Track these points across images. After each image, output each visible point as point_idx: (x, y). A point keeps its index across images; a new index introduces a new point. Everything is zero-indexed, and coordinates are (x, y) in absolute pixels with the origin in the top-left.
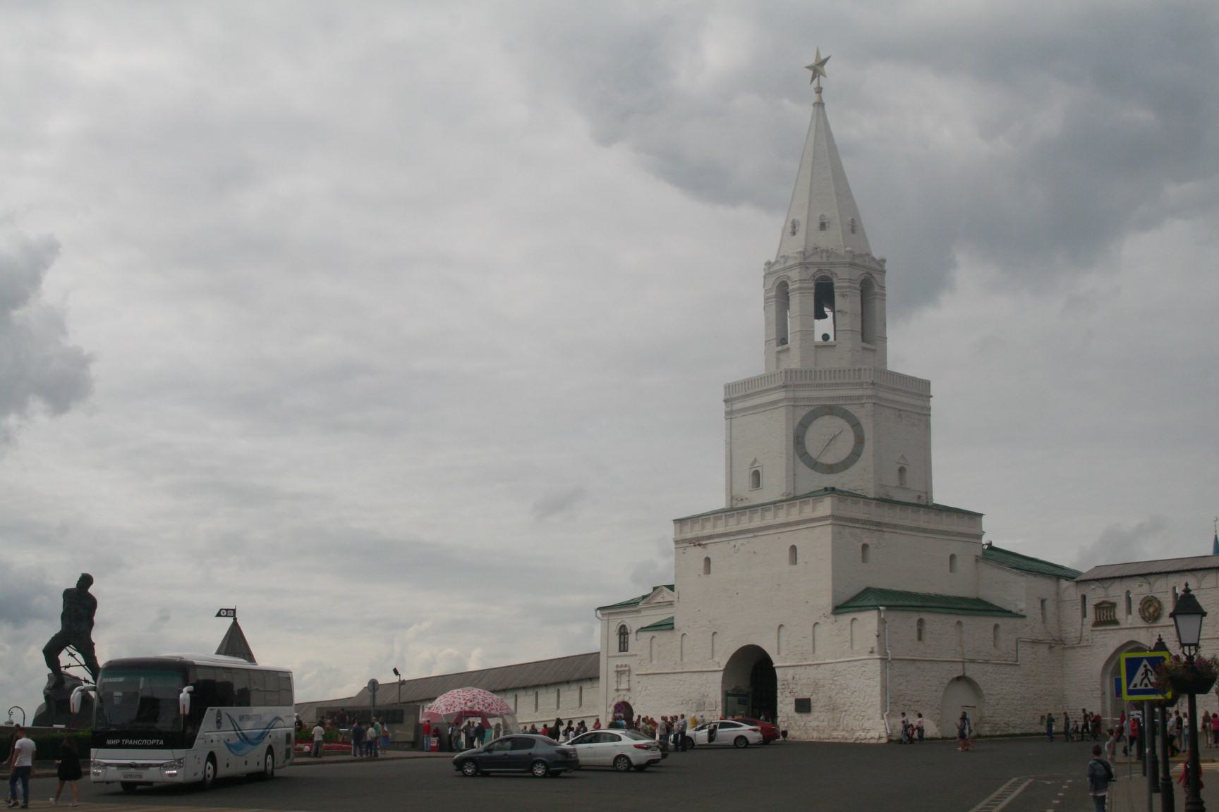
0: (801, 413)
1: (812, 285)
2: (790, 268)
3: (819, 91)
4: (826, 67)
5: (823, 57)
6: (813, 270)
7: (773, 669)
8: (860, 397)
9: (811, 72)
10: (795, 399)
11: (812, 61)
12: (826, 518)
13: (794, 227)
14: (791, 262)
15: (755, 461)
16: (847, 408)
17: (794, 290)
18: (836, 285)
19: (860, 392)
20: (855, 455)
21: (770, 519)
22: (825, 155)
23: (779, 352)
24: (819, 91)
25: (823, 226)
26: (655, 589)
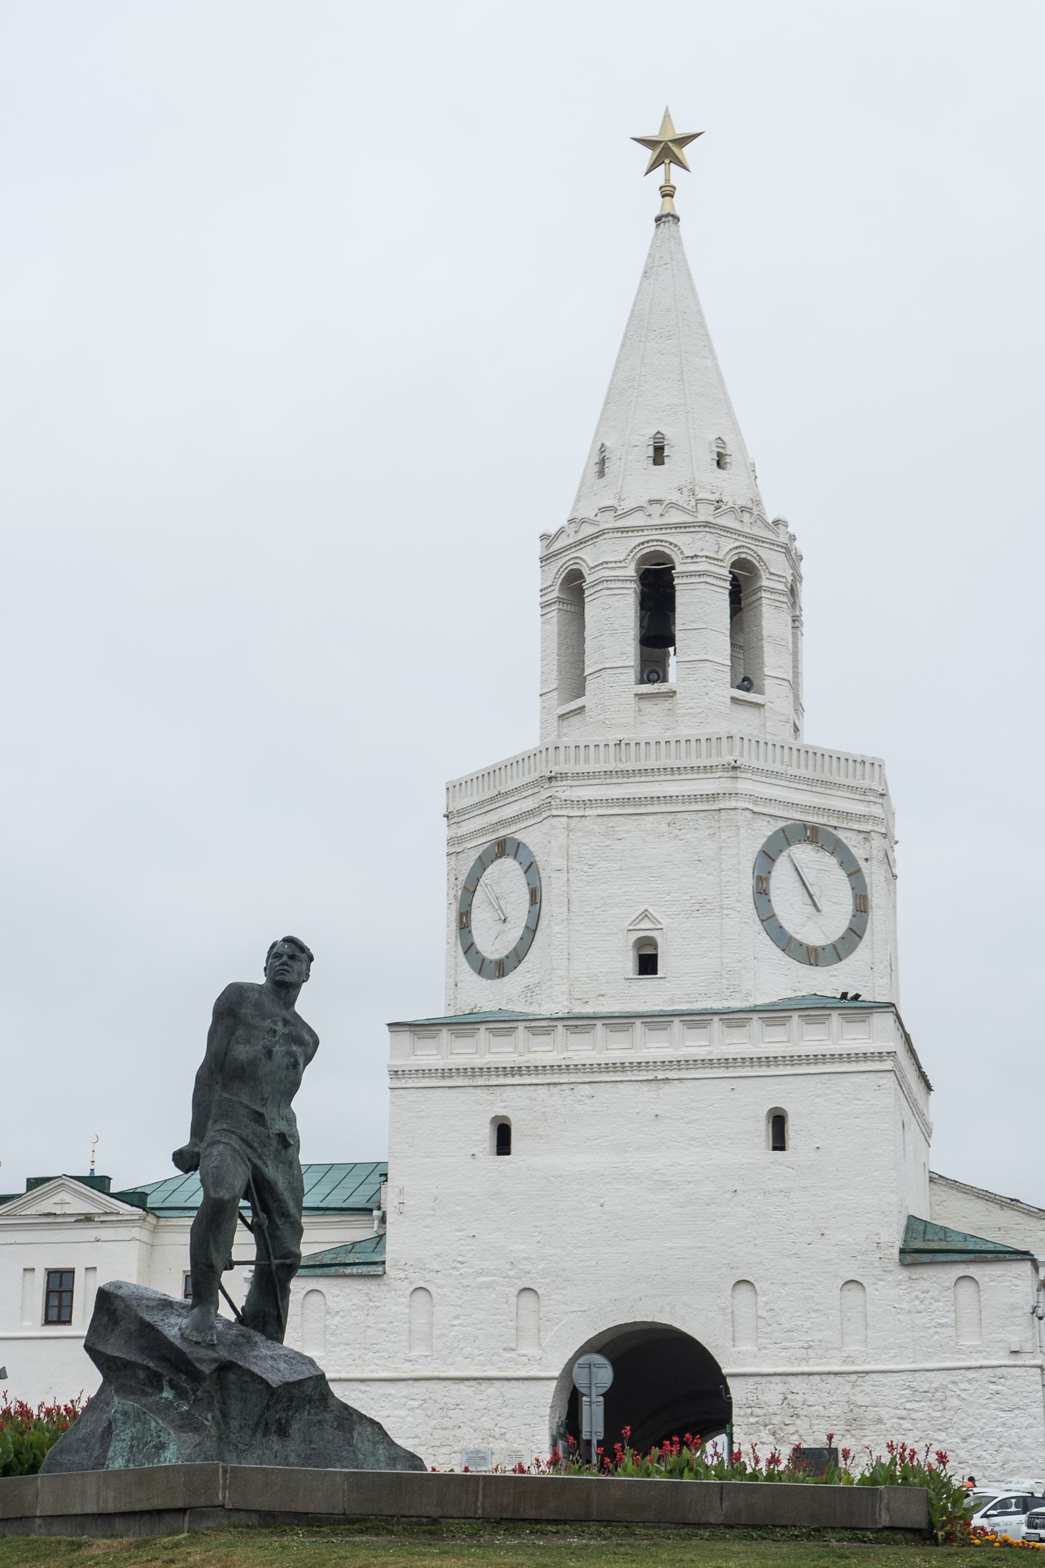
0: (767, 829)
2: (677, 526)
3: (668, 192)
4: (687, 153)
5: (681, 130)
6: (728, 544)
7: (722, 1379)
8: (862, 818)
9: (648, 155)
10: (757, 800)
11: (652, 132)
12: (880, 1056)
14: (676, 517)
15: (645, 915)
16: (841, 835)
18: (765, 583)
20: (855, 933)
21: (695, 1044)
22: (665, 321)
23: (640, 696)
24: (668, 192)
25: (720, 462)
26: (33, 1183)
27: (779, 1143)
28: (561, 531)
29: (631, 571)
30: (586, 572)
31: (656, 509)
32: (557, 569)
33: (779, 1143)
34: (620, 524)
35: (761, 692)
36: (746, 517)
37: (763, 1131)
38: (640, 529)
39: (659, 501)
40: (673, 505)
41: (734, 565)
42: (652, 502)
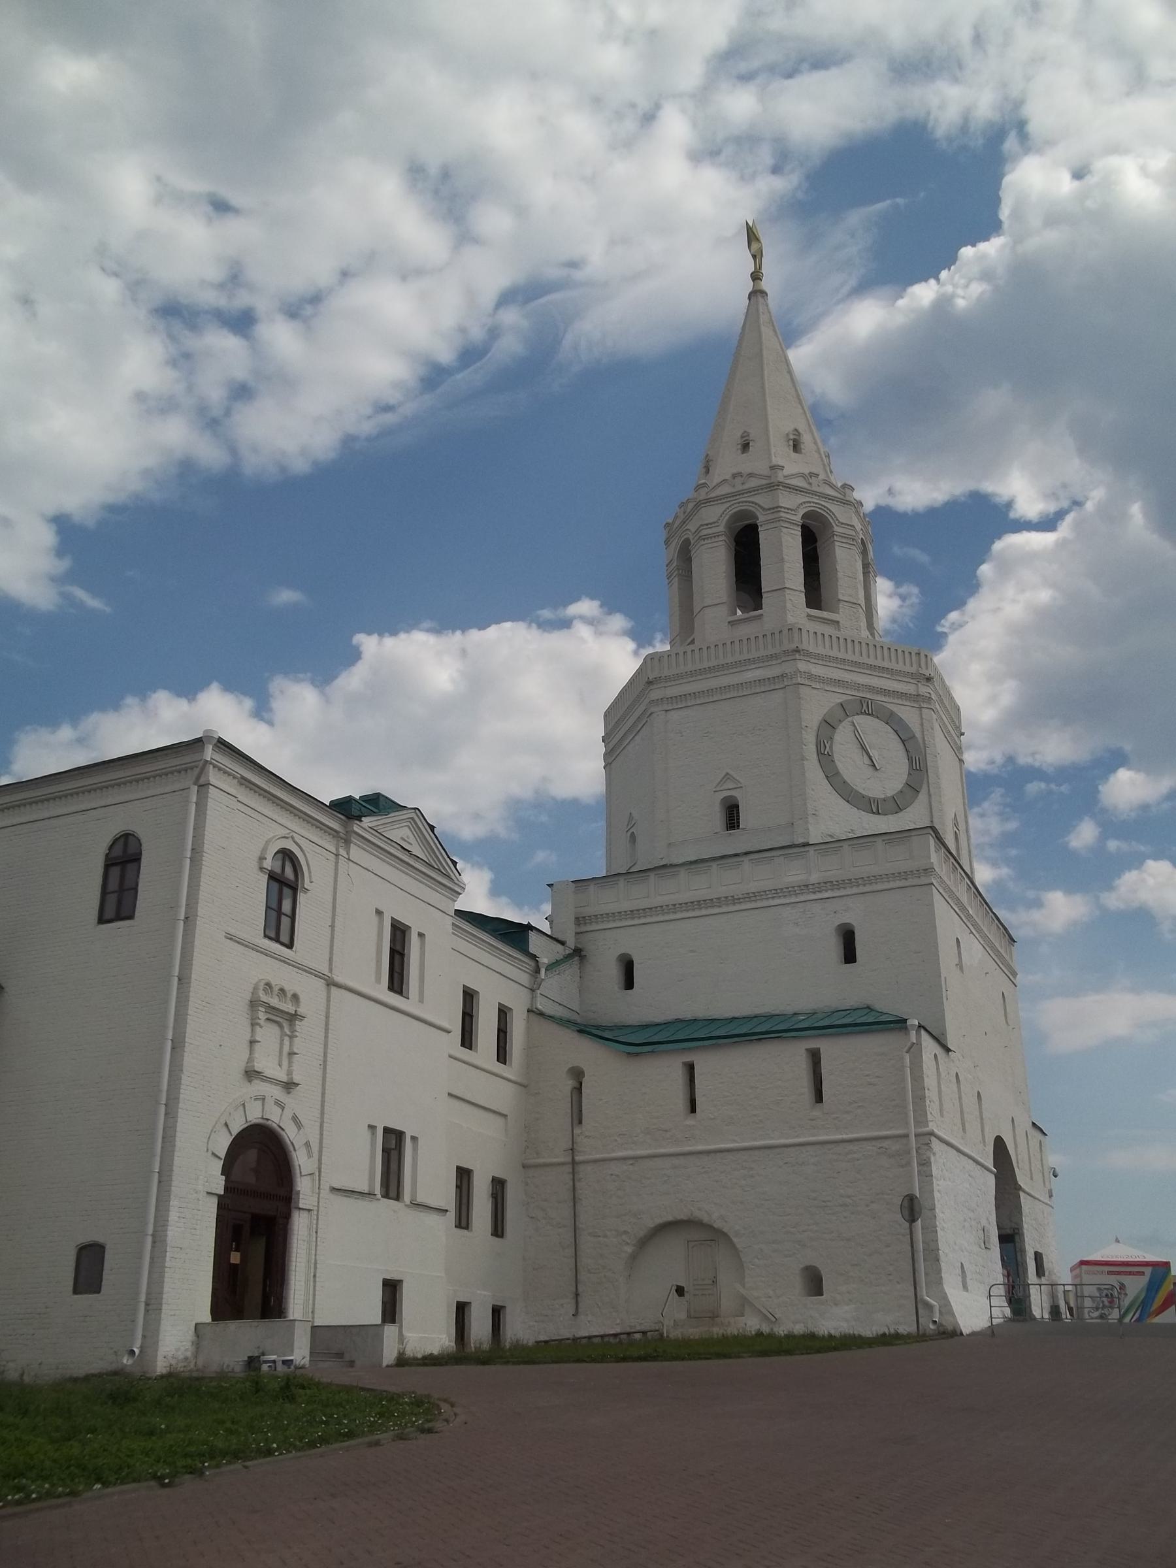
1: (798, 518)
13: (745, 447)
14: (753, 483)
17: (768, 522)
18: (836, 529)
19: (910, 689)
27: (850, 956)
28: (676, 517)
29: (722, 528)
30: (691, 537)
31: (738, 480)
32: (675, 544)
33: (850, 956)
34: (713, 495)
35: (836, 611)
36: (813, 480)
37: (834, 948)
38: (728, 496)
39: (740, 474)
40: (751, 475)
41: (804, 516)
42: (734, 476)
